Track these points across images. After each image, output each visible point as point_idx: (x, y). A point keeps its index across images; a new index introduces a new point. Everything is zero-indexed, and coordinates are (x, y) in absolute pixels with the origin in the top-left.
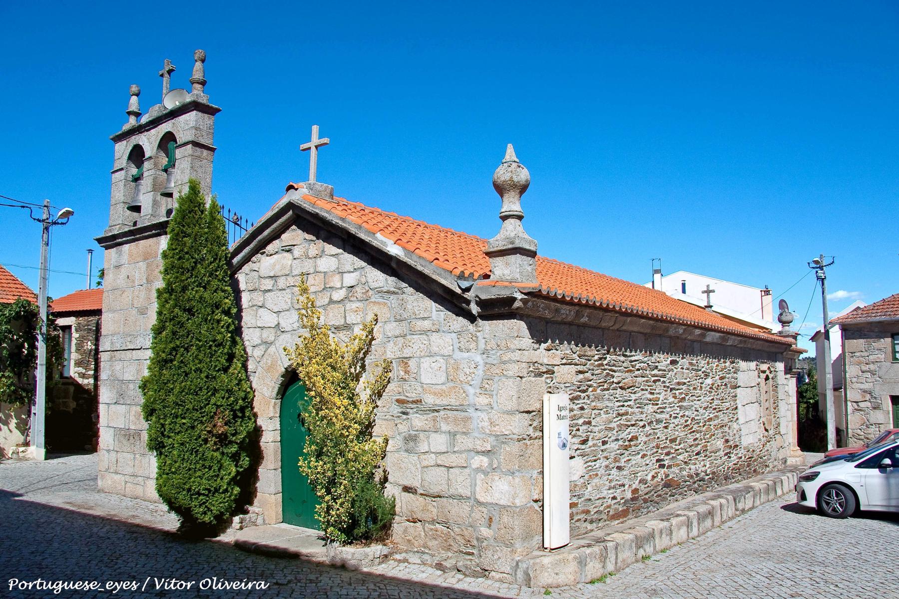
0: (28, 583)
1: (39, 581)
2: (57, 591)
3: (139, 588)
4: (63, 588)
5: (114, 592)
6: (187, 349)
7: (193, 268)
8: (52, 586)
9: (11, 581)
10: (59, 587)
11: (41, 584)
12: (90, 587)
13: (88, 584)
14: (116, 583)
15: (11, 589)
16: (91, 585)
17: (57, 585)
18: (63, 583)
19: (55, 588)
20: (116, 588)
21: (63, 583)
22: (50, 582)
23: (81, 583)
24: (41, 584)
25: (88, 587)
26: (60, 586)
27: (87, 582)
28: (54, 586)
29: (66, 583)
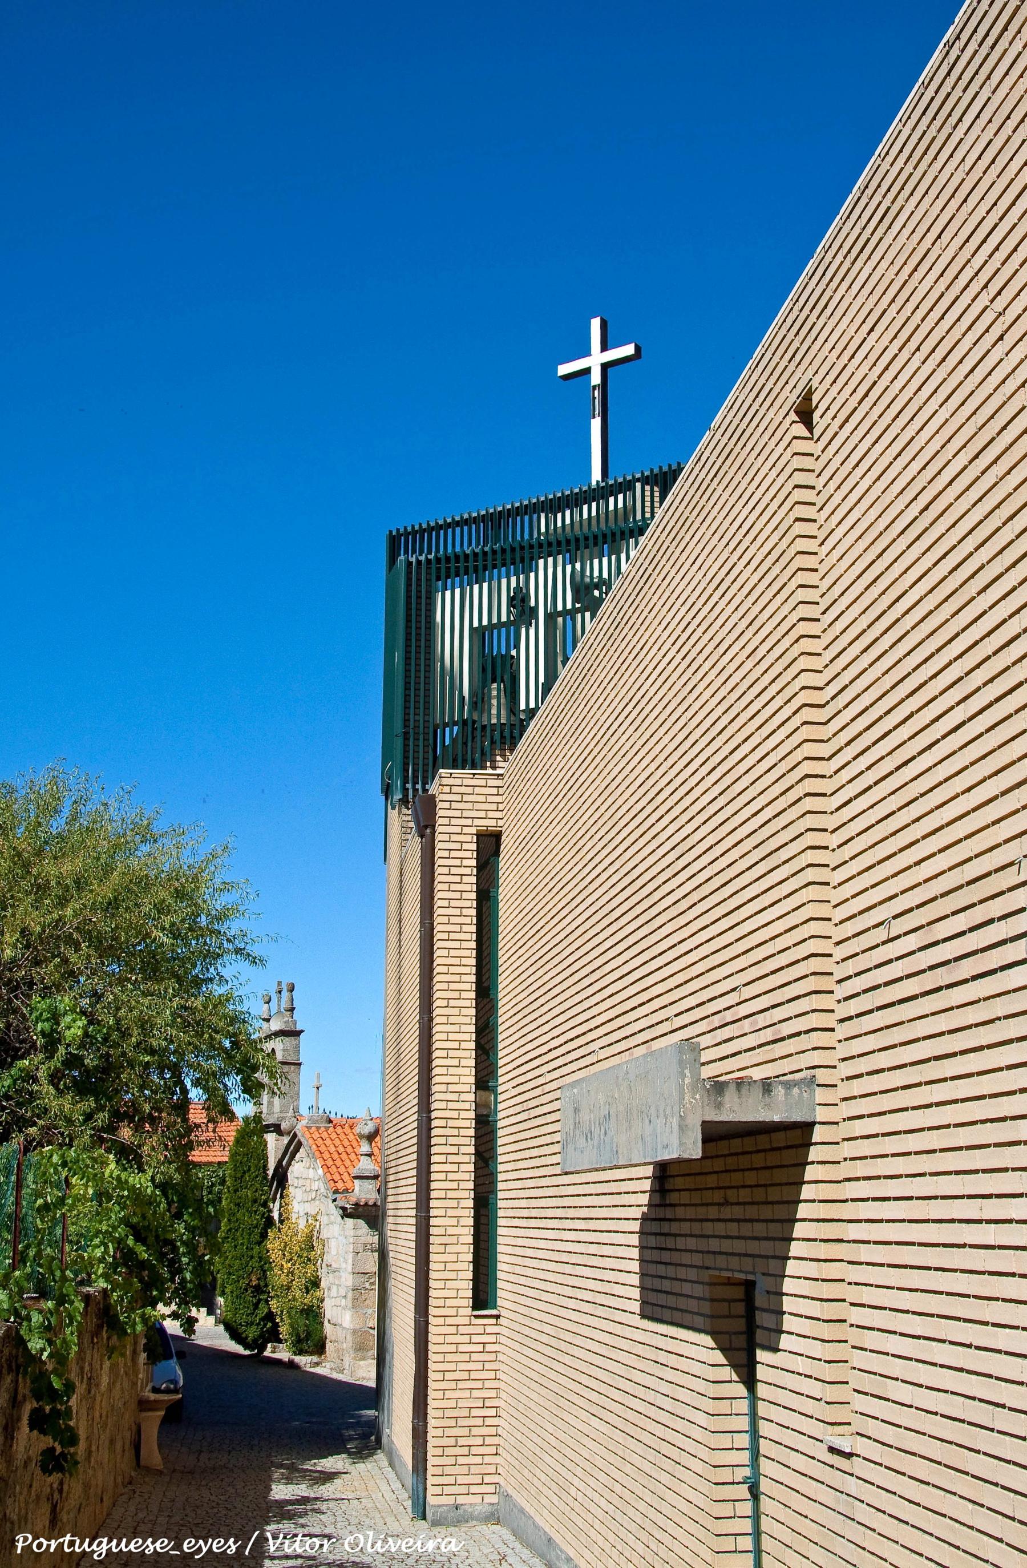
0: (49, 1540)
1: (68, 1537)
2: (100, 1555)
3: (240, 1550)
4: (109, 1550)
5: (197, 1557)
6: (236, 1230)
7: (242, 1177)
8: (89, 1546)
9: (20, 1537)
10: (102, 1547)
11: (72, 1544)
12: (155, 1548)
13: (153, 1543)
14: (201, 1542)
15: (19, 1551)
16: (158, 1545)
17: (98, 1546)
18: (109, 1542)
19: (96, 1549)
20: (200, 1549)
21: (109, 1542)
22: (87, 1540)
23: (141, 1541)
24: (72, 1544)
25: (151, 1548)
26: (104, 1547)
27: (150, 1540)
28: (94, 1547)
29: (115, 1541)
